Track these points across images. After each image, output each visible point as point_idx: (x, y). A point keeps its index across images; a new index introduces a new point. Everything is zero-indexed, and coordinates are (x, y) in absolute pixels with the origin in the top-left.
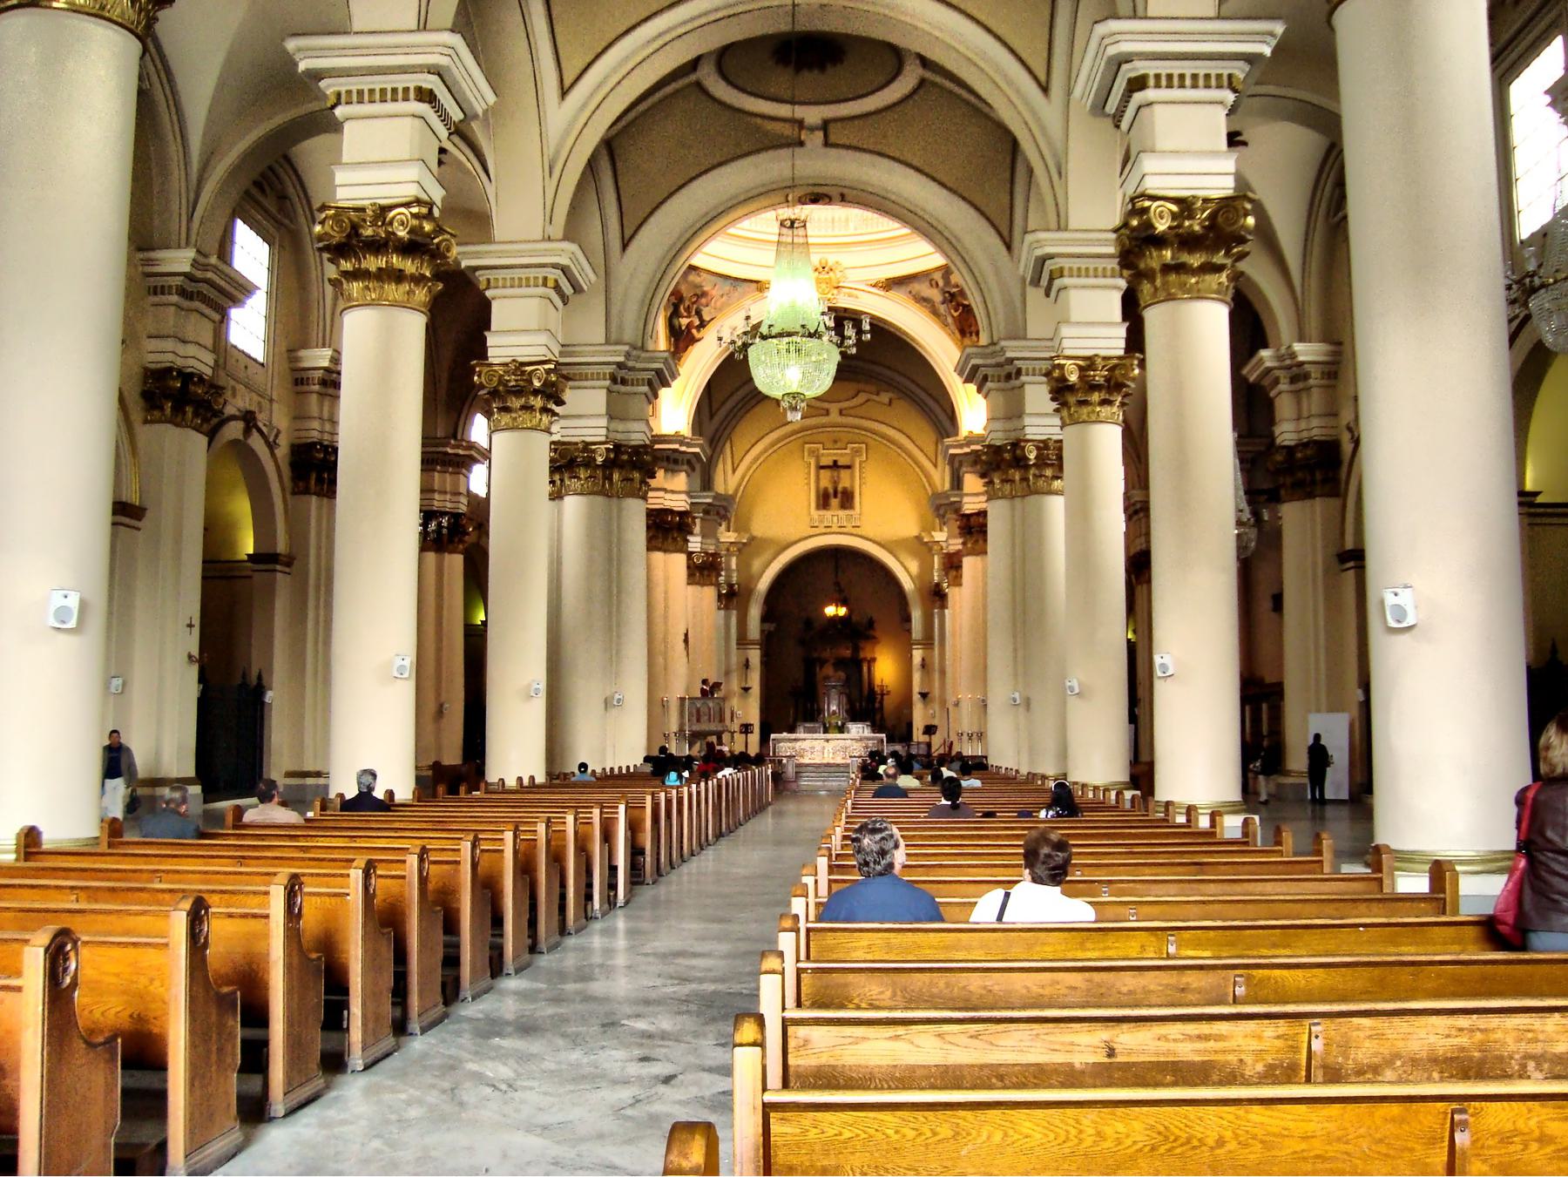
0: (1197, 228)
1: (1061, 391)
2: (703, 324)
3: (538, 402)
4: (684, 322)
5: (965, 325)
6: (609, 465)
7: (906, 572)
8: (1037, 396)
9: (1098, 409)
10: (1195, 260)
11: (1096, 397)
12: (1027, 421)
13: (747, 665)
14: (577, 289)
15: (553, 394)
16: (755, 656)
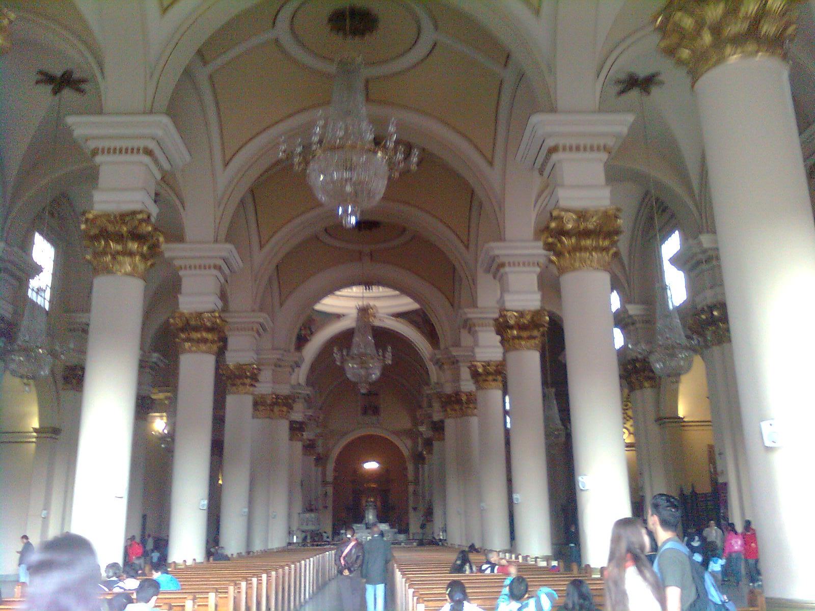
0: (526, 322)
1: (475, 375)
2: (312, 333)
3: (248, 381)
4: (303, 332)
5: (432, 335)
6: (274, 404)
7: (405, 446)
8: (465, 373)
9: (491, 383)
10: (525, 334)
11: (490, 378)
12: (462, 383)
13: (326, 494)
14: (265, 330)
15: (255, 378)
16: (330, 490)
